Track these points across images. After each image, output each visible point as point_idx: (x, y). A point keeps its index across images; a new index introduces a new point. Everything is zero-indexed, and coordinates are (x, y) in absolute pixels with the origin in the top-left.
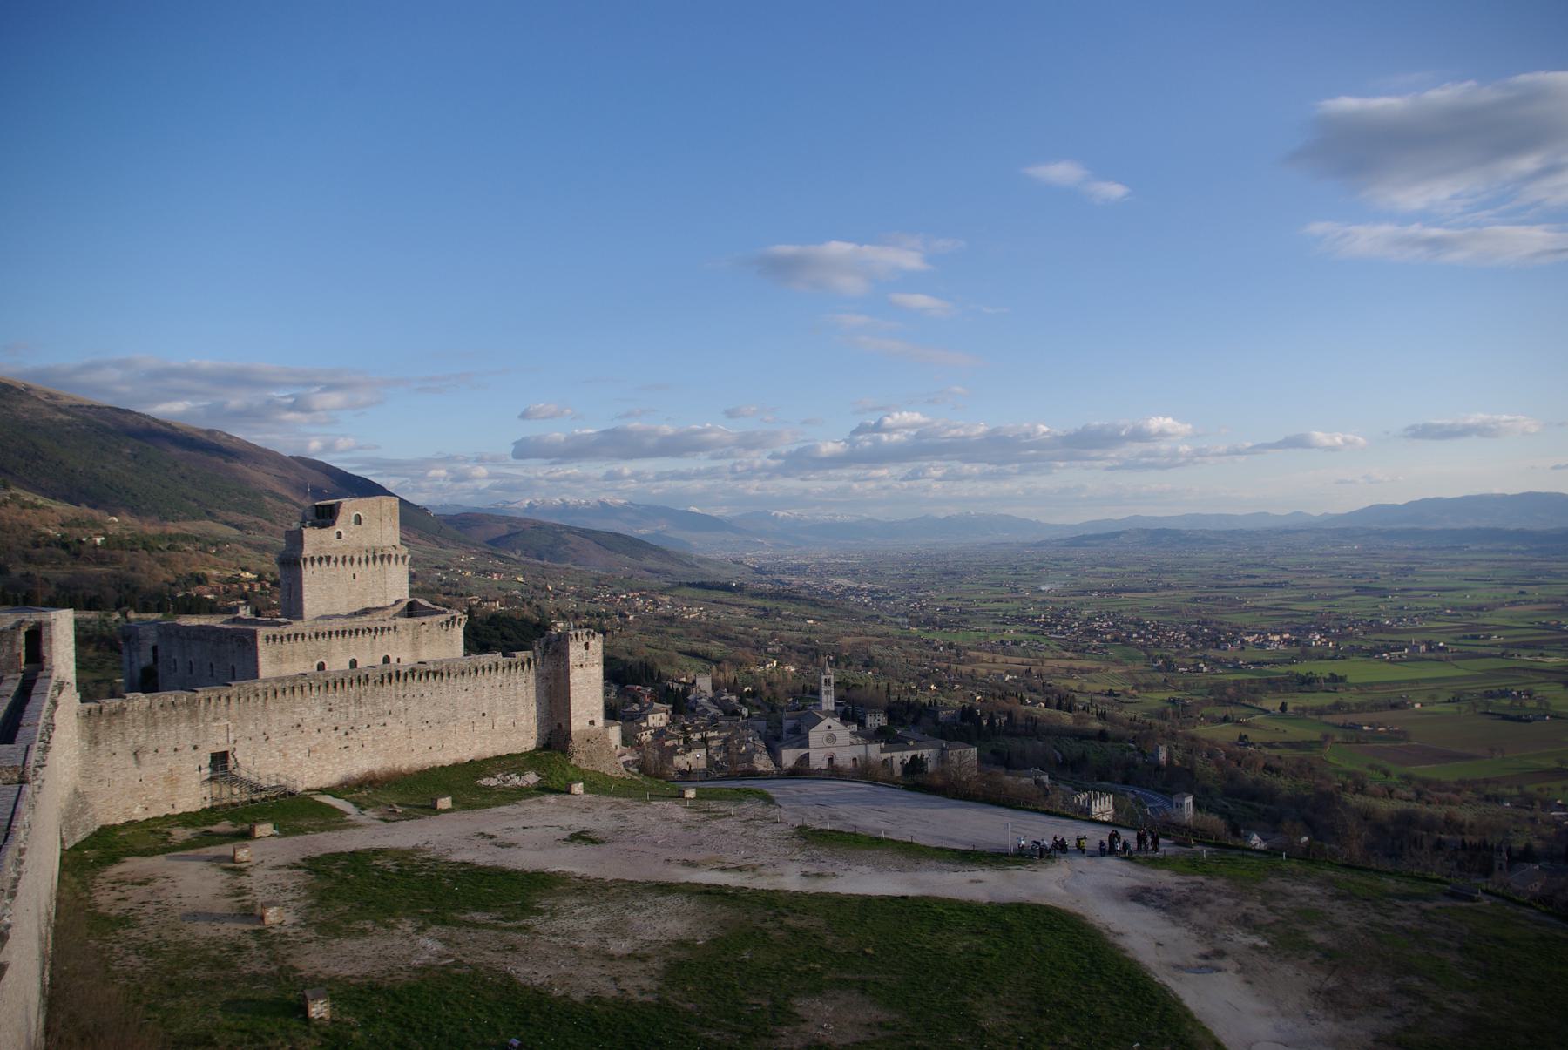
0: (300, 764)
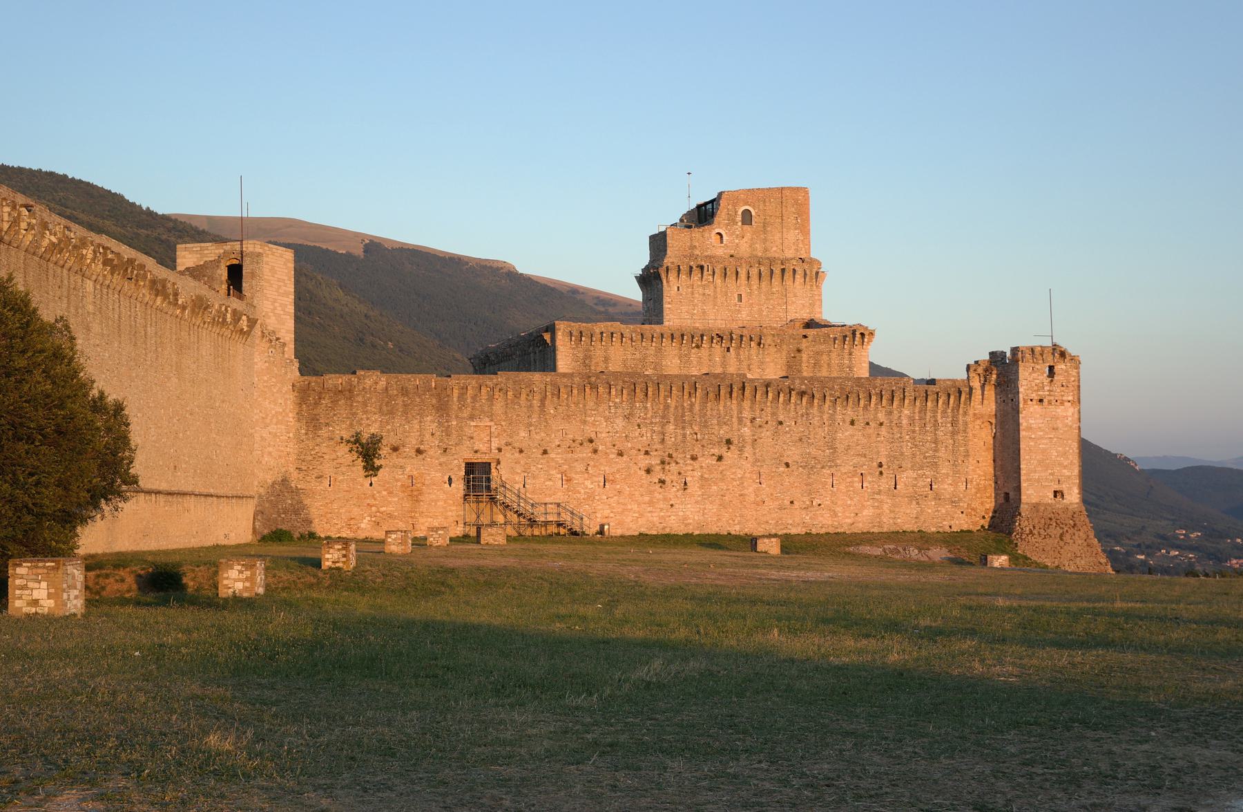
0: (590, 497)
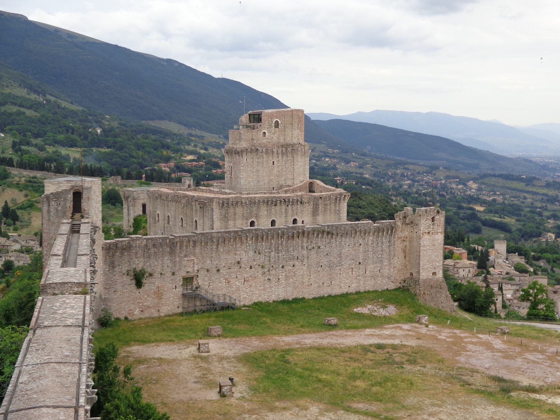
0: (238, 289)
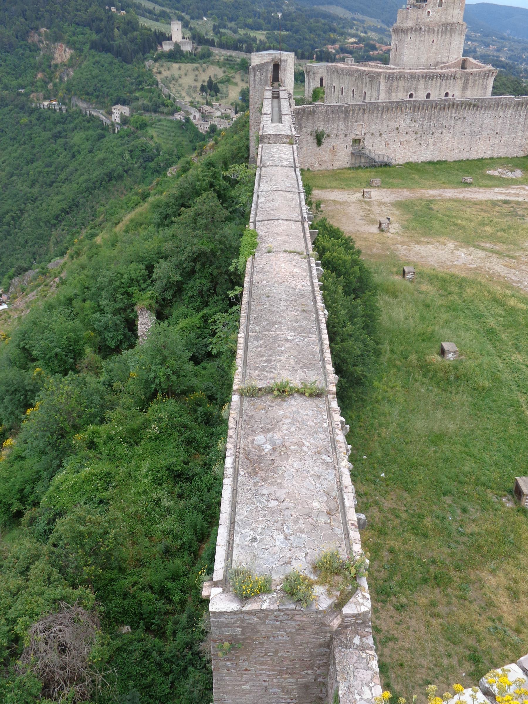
0: (395, 151)
